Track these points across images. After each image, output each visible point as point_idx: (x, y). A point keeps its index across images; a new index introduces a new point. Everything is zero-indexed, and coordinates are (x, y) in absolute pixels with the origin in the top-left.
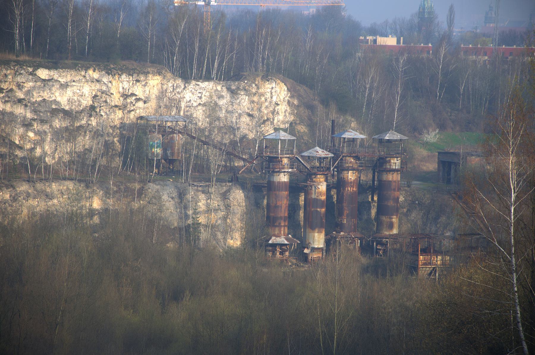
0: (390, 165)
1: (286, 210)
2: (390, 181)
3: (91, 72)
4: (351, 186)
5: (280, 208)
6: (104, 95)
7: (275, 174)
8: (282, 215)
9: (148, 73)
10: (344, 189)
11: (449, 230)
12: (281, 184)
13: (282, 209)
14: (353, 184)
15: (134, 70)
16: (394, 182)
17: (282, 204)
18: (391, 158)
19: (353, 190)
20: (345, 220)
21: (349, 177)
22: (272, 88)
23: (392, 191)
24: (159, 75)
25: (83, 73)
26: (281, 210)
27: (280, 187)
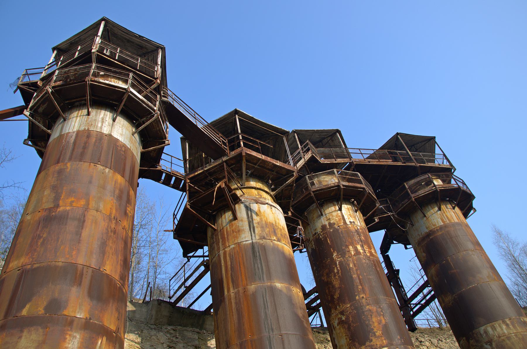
1: (110, 243)
5: (71, 226)
8: (81, 260)
10: (343, 253)
12: (93, 140)
13: (85, 233)
17: (86, 208)
21: (346, 217)
26: (79, 234)
27: (85, 148)
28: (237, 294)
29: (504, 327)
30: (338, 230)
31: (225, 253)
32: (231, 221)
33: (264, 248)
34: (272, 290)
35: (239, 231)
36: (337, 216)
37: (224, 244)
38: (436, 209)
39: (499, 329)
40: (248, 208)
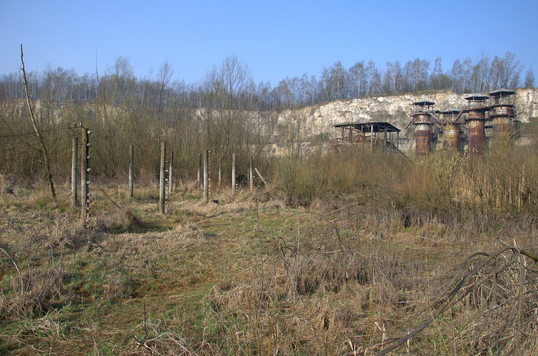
3: (406, 96)
4: (473, 131)
6: (410, 106)
9: (438, 93)
14: (475, 130)
15: (430, 93)
16: (499, 125)
19: (474, 134)
22: (529, 93)
24: (444, 93)
25: (400, 97)
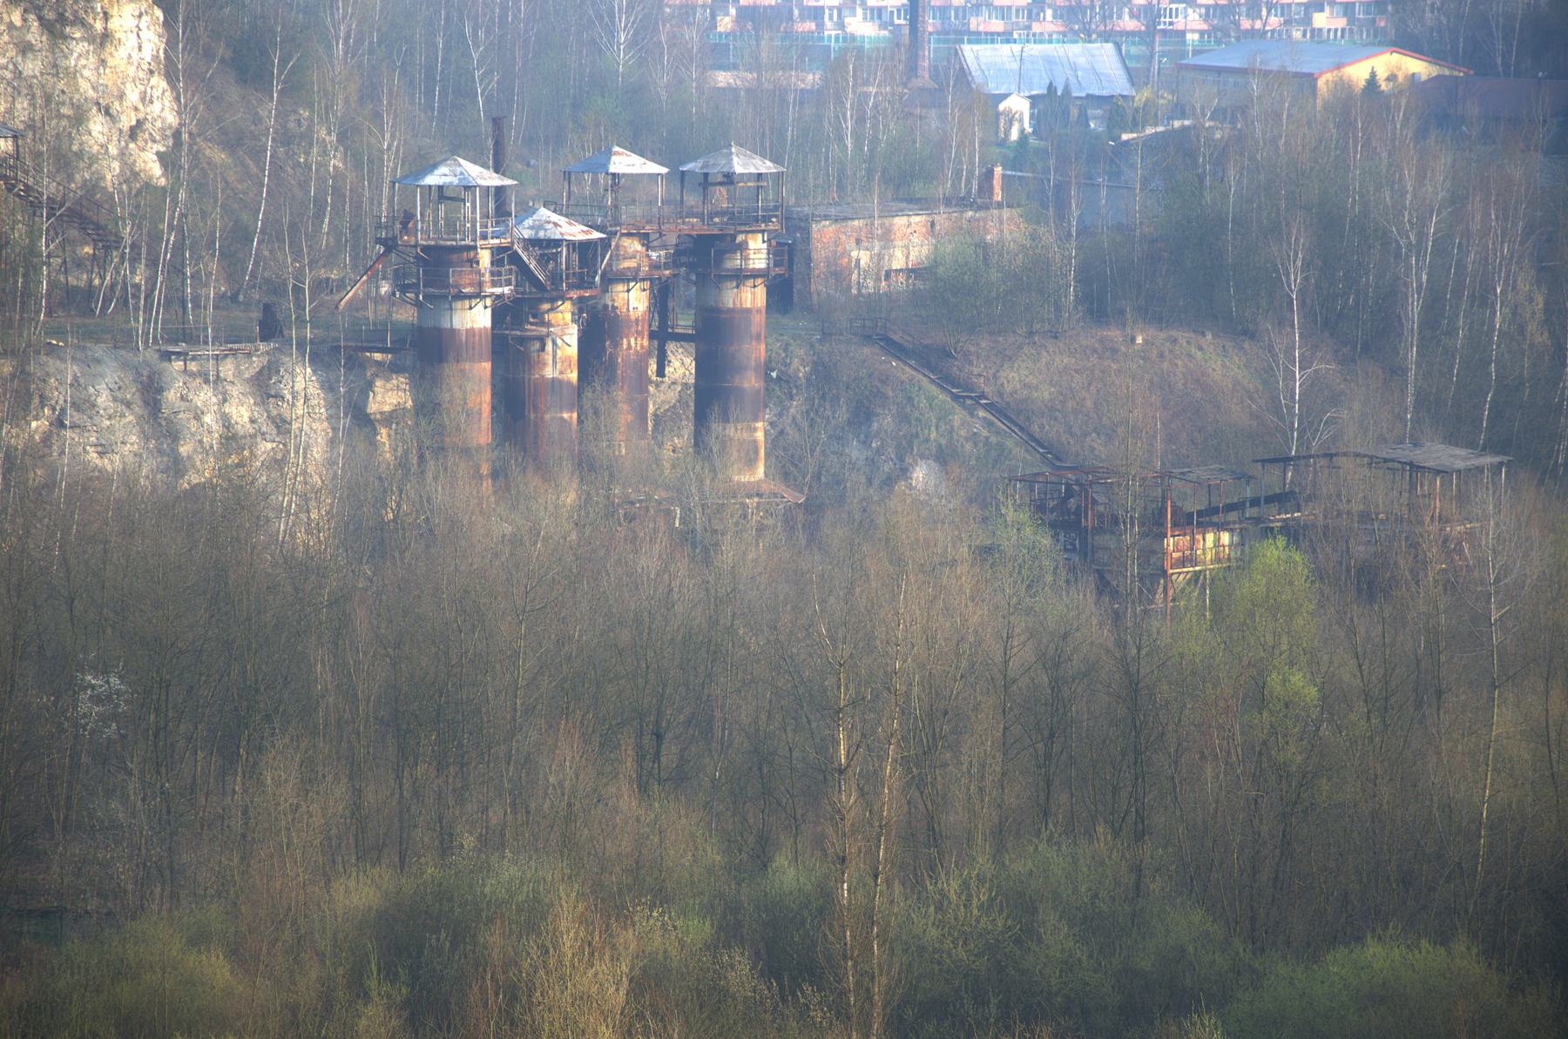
0: (747, 259)
2: (748, 311)
7: (458, 305)
10: (616, 345)
11: (922, 457)
12: (477, 338)
18: (750, 235)
20: (623, 444)
23: (754, 343)
27: (473, 348)
28: (536, 417)
29: (733, 429)
30: (618, 316)
31: (530, 379)
32: (539, 351)
33: (560, 382)
34: (562, 419)
35: (545, 364)
36: (623, 299)
37: (530, 370)
38: (734, 284)
39: (727, 431)
40: (554, 343)
